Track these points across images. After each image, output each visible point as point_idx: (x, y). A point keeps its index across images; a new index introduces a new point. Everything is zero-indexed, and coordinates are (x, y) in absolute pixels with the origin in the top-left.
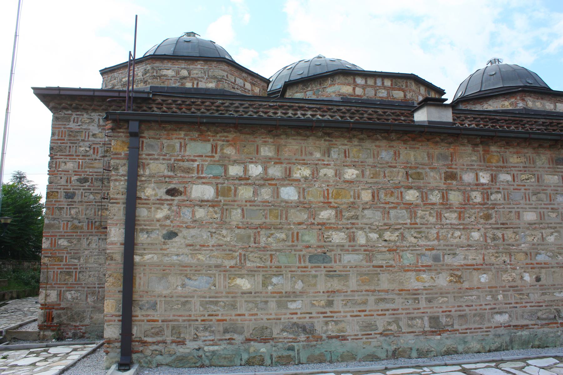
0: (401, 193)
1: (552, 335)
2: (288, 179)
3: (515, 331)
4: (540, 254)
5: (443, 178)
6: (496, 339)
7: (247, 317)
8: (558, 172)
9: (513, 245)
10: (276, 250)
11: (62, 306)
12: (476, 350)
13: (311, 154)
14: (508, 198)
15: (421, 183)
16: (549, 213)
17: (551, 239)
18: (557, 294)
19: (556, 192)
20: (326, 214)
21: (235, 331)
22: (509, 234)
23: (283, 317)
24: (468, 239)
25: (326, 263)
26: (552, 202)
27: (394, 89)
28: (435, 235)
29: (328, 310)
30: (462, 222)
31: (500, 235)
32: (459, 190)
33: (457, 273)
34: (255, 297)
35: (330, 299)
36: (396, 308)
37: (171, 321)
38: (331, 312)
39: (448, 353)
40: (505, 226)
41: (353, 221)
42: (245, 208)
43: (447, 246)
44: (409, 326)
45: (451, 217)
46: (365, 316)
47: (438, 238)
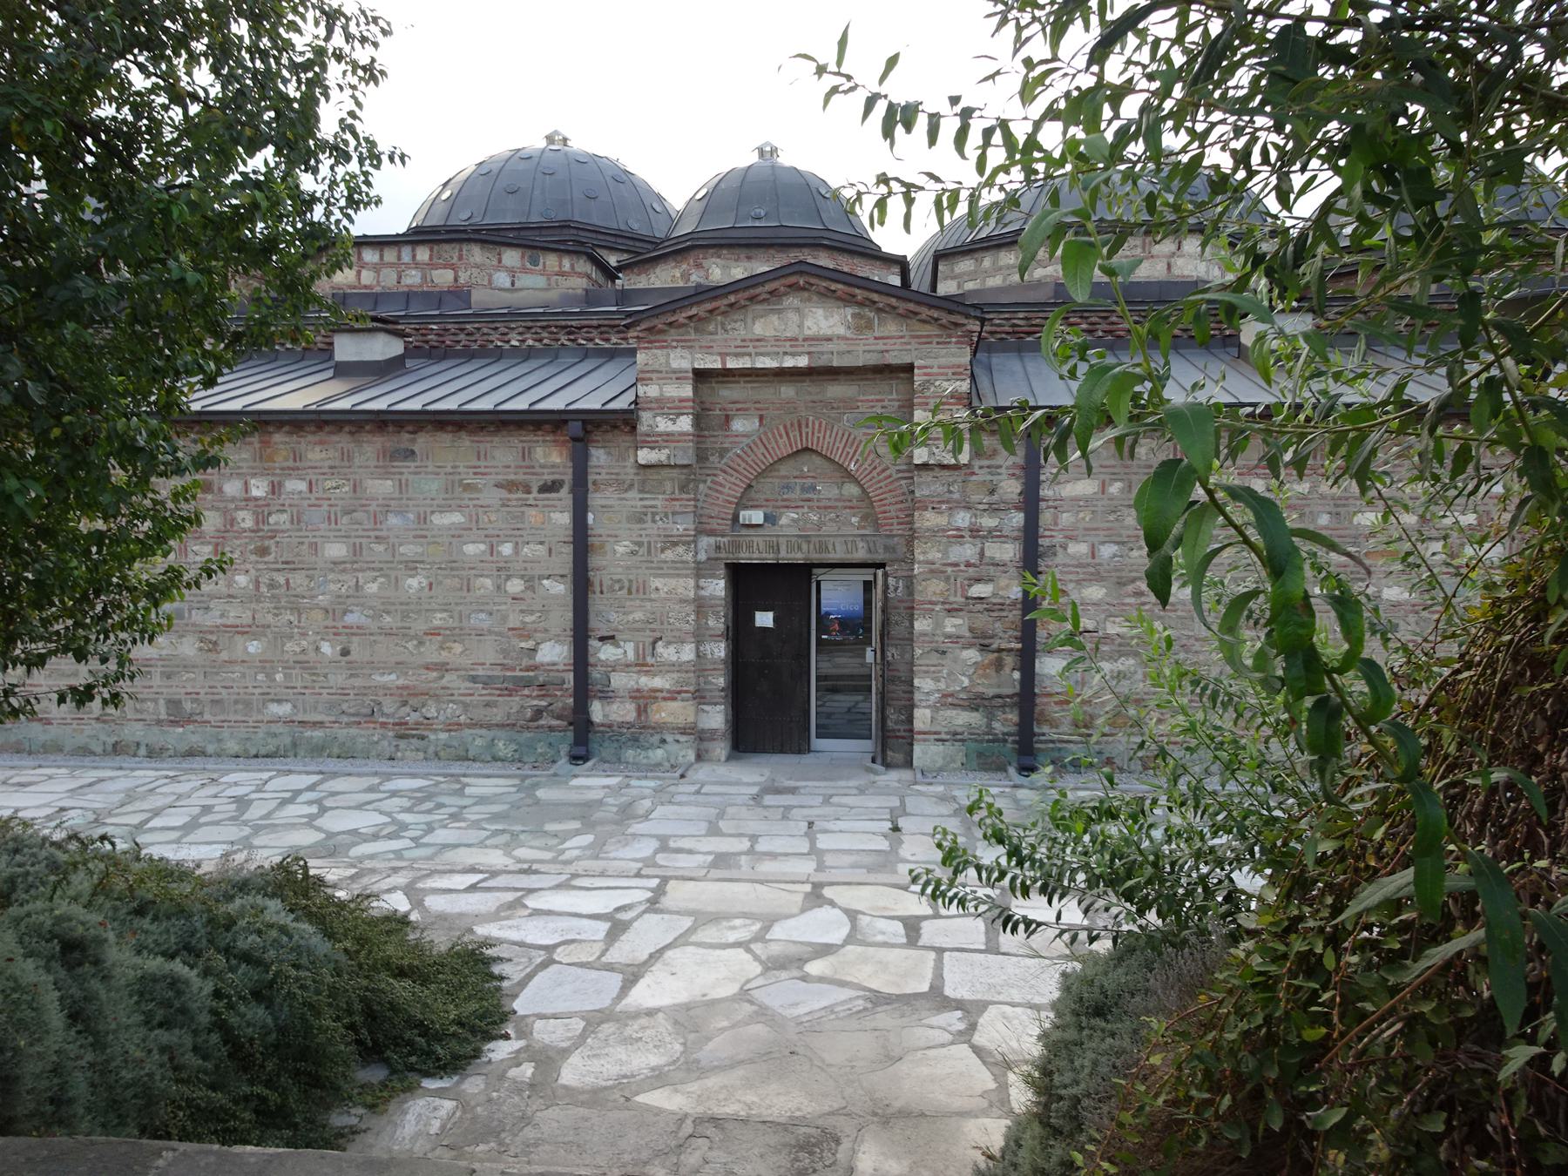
17: (372, 588)
18: (378, 678)
22: (298, 579)
24: (229, 586)
27: (435, 267)
31: (282, 581)
32: (218, 509)
39: (191, 753)
40: (289, 566)
44: (137, 710)
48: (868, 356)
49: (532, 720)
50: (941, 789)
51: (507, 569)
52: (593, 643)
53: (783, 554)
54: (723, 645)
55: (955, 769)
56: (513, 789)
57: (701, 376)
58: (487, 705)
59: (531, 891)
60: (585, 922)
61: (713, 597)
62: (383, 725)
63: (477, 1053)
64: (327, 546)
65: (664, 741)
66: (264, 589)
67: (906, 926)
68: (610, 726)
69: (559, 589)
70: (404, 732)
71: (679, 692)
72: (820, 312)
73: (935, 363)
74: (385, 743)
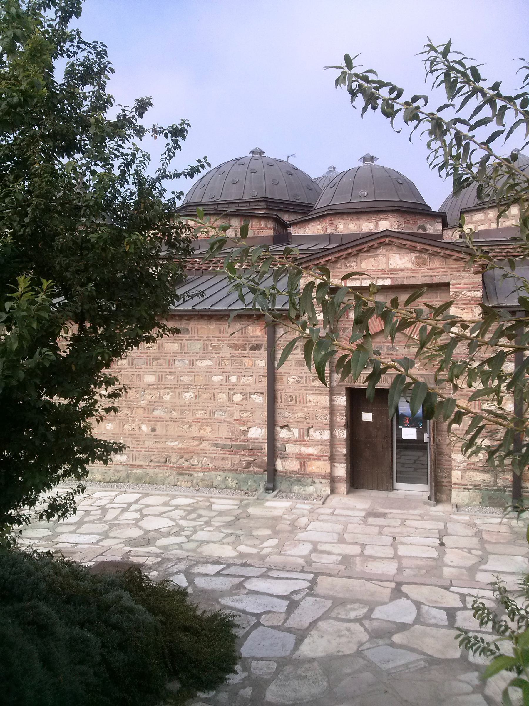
1: (161, 475)
3: (131, 469)
4: (157, 409)
6: (116, 474)
8: (179, 340)
9: (134, 402)
14: (132, 364)
16: (167, 376)
17: (167, 398)
18: (168, 443)
19: (175, 358)
48: (424, 279)
49: (246, 468)
50: (467, 518)
51: (234, 389)
52: (278, 429)
54: (345, 431)
55: (475, 506)
56: (236, 507)
58: (223, 459)
59: (247, 578)
60: (276, 600)
61: (339, 406)
62: (172, 467)
63: (222, 680)
64: (146, 376)
67: (448, 614)
68: (286, 473)
69: (260, 400)
70: (181, 472)
71: (322, 456)
72: (397, 256)
73: (463, 281)
74: (172, 477)
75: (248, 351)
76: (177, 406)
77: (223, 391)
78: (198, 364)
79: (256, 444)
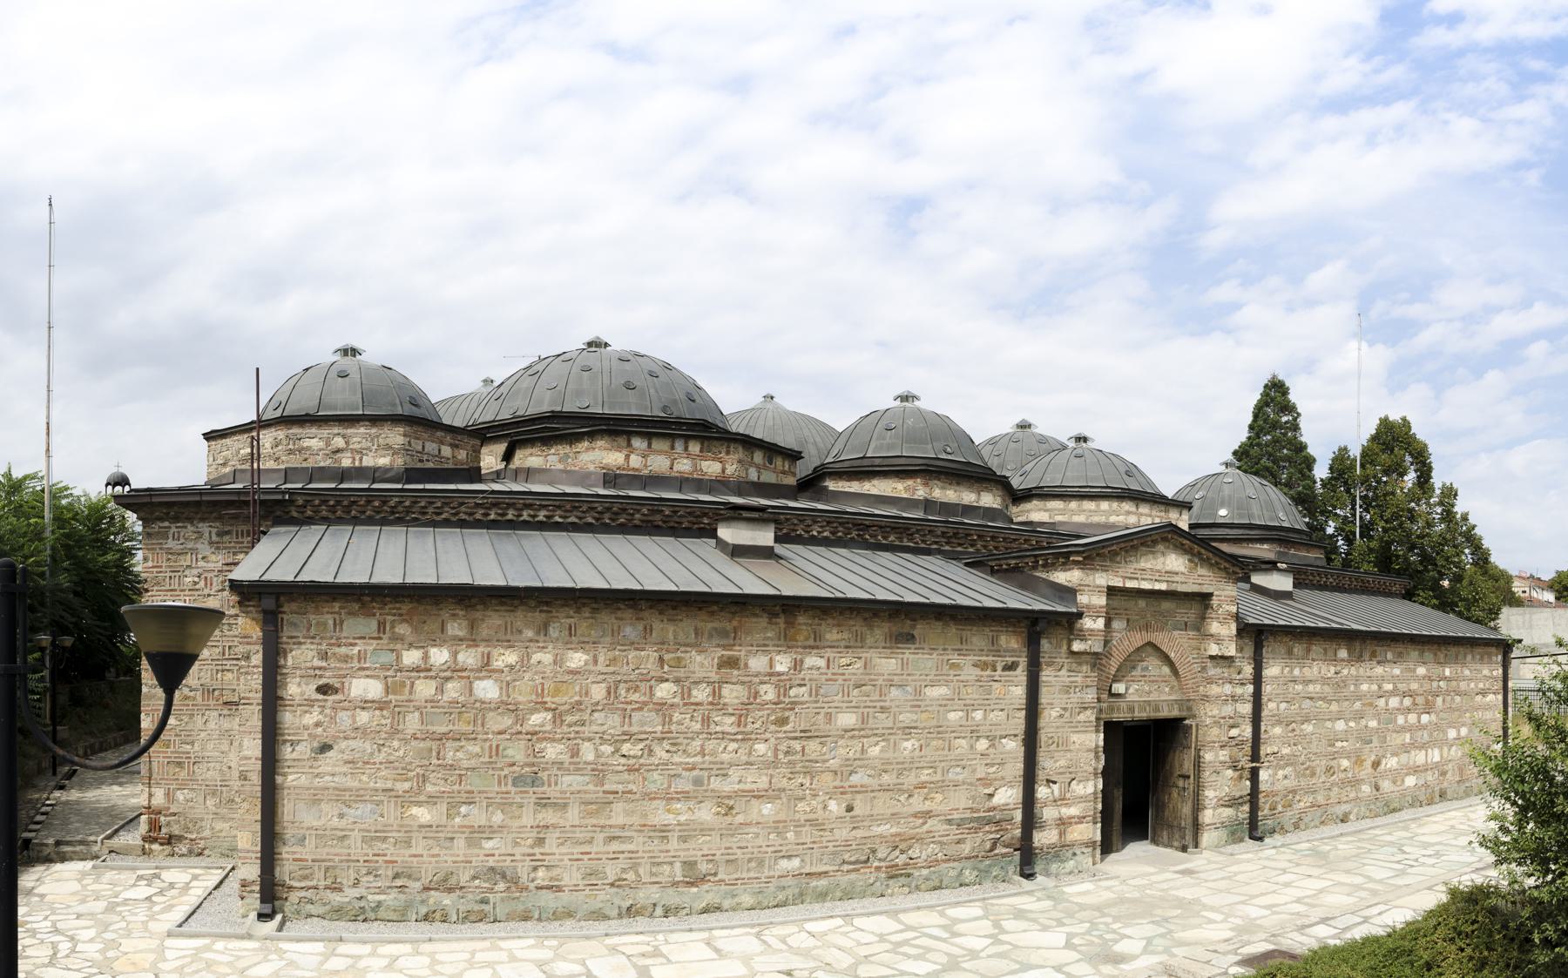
0: (651, 687)
2: (486, 668)
4: (856, 772)
5: (715, 666)
7: (425, 858)
9: (817, 762)
10: (467, 769)
11: (171, 811)
12: (749, 906)
13: (520, 632)
15: (681, 673)
17: (875, 751)
20: (536, 719)
21: (409, 877)
22: (813, 746)
23: (474, 859)
25: (537, 786)
26: (883, 698)
28: (699, 749)
29: (537, 850)
30: (742, 729)
31: (798, 748)
32: (743, 683)
33: (727, 802)
34: (437, 832)
35: (541, 836)
36: (636, 849)
37: (323, 861)
38: (542, 854)
40: (806, 735)
41: (577, 729)
42: (424, 710)
43: (714, 763)
44: (652, 874)
45: (727, 723)
46: (589, 859)
47: (702, 753)
49: (991, 850)
53: (1136, 714)
57: (1112, 591)
62: (878, 868)
64: (840, 715)
65: (1075, 854)
66: (781, 756)
74: (878, 884)
75: (999, 672)
76: (891, 764)
77: (963, 735)
78: (928, 694)
79: (1005, 812)
